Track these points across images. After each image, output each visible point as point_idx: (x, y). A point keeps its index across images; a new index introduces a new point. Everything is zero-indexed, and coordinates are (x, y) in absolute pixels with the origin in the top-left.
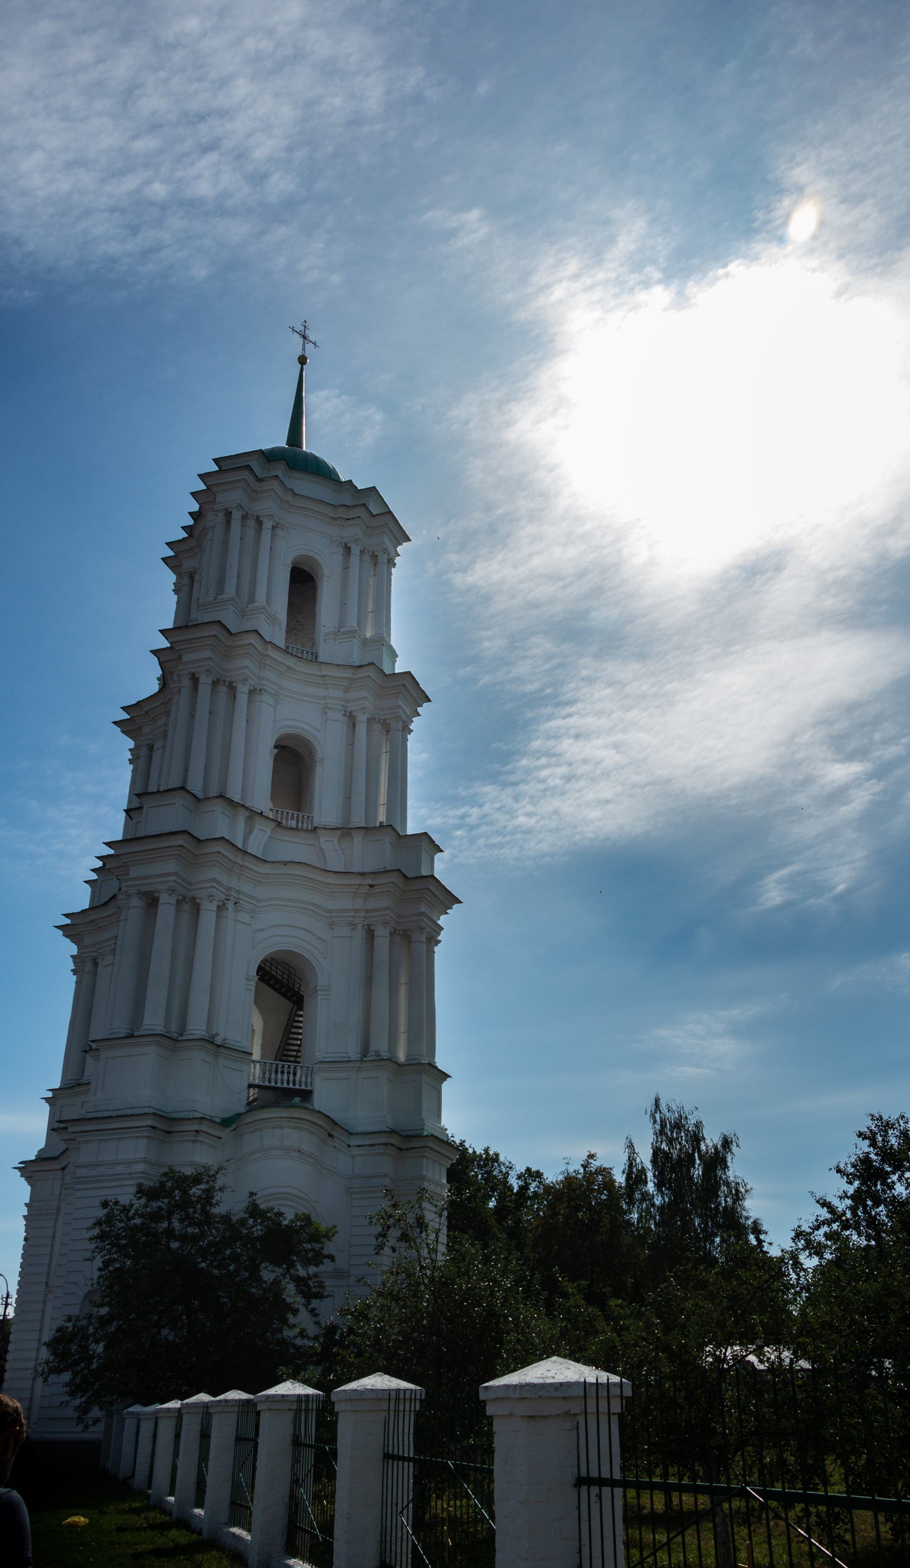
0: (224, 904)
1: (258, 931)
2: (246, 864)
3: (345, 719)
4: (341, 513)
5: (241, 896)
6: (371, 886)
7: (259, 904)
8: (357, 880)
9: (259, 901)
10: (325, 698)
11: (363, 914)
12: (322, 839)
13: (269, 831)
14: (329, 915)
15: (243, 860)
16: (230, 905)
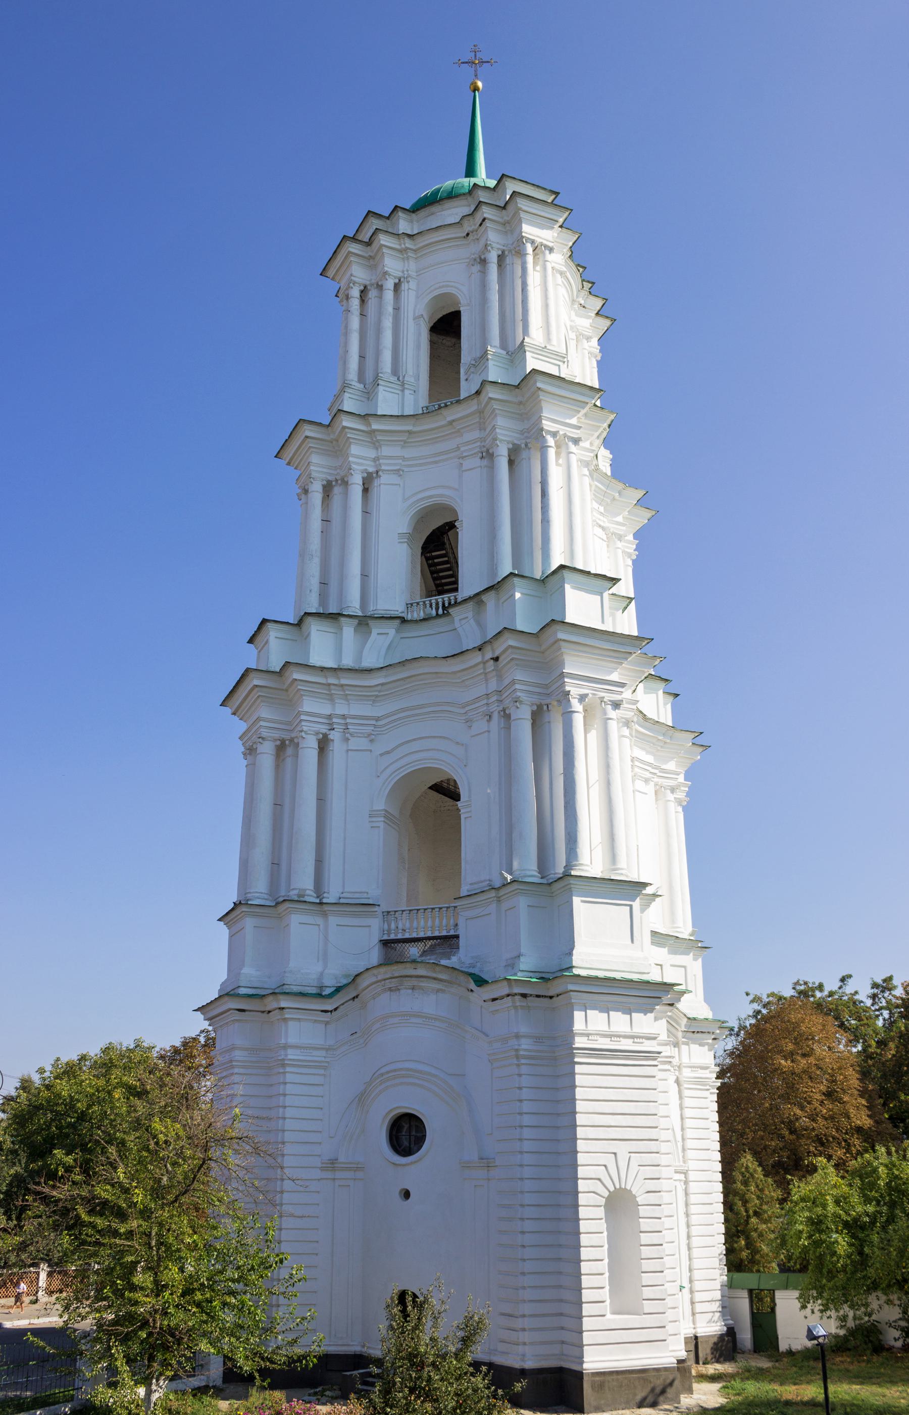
0: (325, 736)
1: (381, 755)
2: (344, 681)
3: (485, 462)
4: (467, 227)
5: (348, 721)
6: (496, 659)
7: (380, 723)
8: (477, 658)
9: (378, 719)
10: (458, 448)
11: (494, 698)
12: (457, 619)
13: (392, 632)
14: (463, 711)
15: (339, 678)
16: (335, 736)
